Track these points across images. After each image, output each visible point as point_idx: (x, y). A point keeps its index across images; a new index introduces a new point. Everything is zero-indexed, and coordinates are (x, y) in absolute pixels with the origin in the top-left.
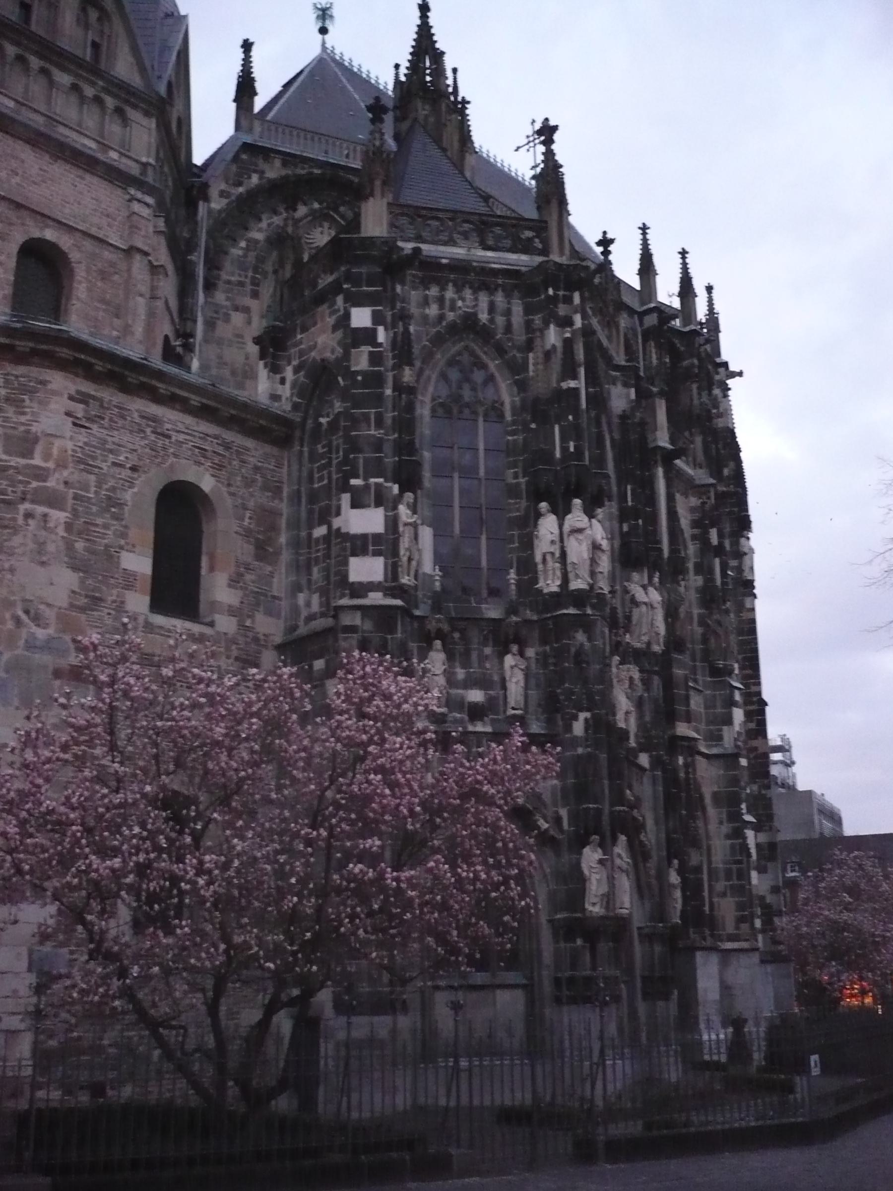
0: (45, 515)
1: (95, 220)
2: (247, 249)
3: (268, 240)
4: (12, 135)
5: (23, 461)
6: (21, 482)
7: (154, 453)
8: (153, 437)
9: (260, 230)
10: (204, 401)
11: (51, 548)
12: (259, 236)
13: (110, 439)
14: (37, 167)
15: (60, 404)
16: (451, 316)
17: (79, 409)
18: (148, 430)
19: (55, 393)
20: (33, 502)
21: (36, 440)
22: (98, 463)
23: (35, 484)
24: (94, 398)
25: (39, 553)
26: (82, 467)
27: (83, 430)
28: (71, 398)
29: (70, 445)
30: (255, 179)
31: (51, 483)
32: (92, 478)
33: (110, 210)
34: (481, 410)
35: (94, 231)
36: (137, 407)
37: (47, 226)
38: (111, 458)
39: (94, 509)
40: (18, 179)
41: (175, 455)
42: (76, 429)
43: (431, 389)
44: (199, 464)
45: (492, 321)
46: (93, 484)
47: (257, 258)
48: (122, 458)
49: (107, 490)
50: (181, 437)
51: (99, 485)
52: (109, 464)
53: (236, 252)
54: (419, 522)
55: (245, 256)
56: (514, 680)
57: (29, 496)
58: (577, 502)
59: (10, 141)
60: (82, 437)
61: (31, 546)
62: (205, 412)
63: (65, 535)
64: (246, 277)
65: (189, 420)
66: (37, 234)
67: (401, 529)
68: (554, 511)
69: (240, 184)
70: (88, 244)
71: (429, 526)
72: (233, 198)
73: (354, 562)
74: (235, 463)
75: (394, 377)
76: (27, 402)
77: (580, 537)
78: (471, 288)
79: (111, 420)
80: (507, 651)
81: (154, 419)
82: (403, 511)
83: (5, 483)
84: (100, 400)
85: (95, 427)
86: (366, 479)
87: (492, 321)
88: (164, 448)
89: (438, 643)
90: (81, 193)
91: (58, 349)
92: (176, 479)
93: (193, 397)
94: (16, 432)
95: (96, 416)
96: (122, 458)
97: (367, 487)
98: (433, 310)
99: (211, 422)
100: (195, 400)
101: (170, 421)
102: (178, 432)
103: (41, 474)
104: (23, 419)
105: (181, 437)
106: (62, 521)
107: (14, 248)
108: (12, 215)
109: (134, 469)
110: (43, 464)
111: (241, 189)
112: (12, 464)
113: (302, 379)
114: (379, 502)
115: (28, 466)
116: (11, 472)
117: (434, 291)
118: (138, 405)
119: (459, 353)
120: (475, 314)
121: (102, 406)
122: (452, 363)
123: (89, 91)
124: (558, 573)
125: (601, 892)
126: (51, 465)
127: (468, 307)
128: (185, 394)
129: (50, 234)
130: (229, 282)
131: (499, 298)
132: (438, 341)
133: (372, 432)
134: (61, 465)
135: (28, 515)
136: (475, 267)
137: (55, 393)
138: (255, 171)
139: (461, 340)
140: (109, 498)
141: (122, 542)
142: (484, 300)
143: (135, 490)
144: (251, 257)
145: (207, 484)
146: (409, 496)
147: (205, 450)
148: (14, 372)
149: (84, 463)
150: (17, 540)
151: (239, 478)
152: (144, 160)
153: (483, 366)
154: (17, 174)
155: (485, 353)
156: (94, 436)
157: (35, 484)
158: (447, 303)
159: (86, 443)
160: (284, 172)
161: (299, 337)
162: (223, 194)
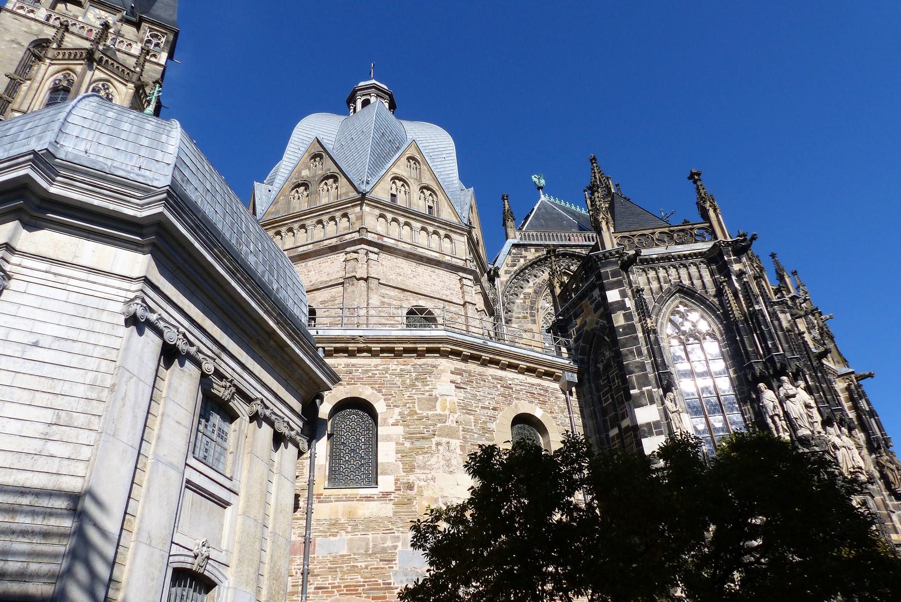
0: (448, 443)
1: (445, 292)
2: (525, 297)
3: (535, 292)
5: (430, 413)
6: (431, 425)
8: (502, 389)
9: (530, 287)
10: (528, 364)
11: (454, 462)
12: (531, 291)
14: (410, 270)
15: (448, 377)
16: (666, 286)
17: (458, 378)
18: (499, 386)
19: (443, 371)
20: (439, 436)
21: (437, 399)
24: (465, 371)
25: (448, 466)
26: (464, 411)
27: (462, 390)
28: (452, 373)
29: (456, 400)
30: (522, 261)
31: (448, 423)
32: (472, 417)
33: (451, 286)
35: (444, 298)
36: (490, 373)
37: (420, 299)
38: (480, 405)
39: (476, 436)
40: (401, 277)
41: (517, 399)
42: (459, 390)
44: (531, 402)
47: (531, 303)
48: (487, 404)
51: (476, 422)
52: (480, 408)
53: (519, 301)
54: (680, 410)
55: (525, 302)
57: (436, 433)
60: (461, 394)
61: (443, 462)
63: (462, 453)
64: (527, 313)
67: (671, 415)
68: (770, 387)
69: (515, 265)
70: (441, 304)
72: (513, 273)
73: (644, 441)
74: (552, 399)
75: (642, 326)
76: (428, 378)
81: (501, 379)
82: (668, 403)
83: (422, 427)
84: (469, 372)
85: (468, 387)
87: (692, 283)
90: (435, 279)
91: (440, 345)
94: (423, 396)
95: (468, 381)
97: (642, 393)
101: (510, 379)
103: (442, 419)
104: (427, 388)
105: (518, 388)
106: (458, 444)
109: (494, 409)
110: (442, 413)
111: (516, 268)
112: (425, 414)
113: (581, 344)
114: (652, 402)
115: (434, 415)
116: (424, 420)
118: (492, 371)
121: (470, 375)
123: (431, 229)
126: (447, 412)
127: (675, 279)
129: (423, 303)
130: (519, 318)
131: (693, 269)
134: (453, 412)
137: (443, 371)
138: (521, 257)
142: (683, 272)
143: (498, 421)
144: (528, 302)
148: (419, 363)
149: (466, 409)
150: (434, 460)
151: (556, 408)
152: (464, 258)
157: (439, 425)
158: (662, 280)
160: (537, 255)
161: (574, 321)
162: (506, 272)
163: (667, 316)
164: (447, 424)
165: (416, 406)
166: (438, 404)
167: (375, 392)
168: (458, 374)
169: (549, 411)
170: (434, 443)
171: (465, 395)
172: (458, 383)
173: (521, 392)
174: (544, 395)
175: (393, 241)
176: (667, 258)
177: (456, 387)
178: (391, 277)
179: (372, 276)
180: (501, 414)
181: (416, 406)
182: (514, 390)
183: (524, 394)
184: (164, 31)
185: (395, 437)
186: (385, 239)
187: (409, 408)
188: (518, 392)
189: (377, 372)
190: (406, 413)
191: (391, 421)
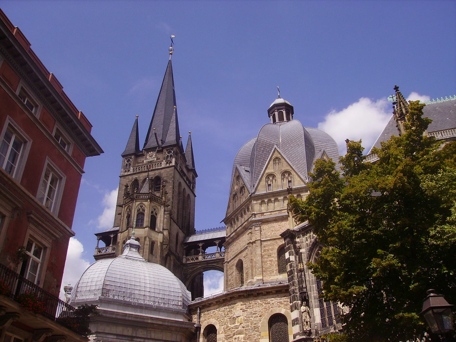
0: (238, 337)
5: (233, 325)
7: (265, 310)
13: (253, 311)
14: (278, 226)
18: (263, 304)
20: (236, 335)
22: (251, 318)
23: (236, 330)
27: (246, 312)
32: (250, 323)
46: (250, 325)
49: (254, 325)
60: (245, 314)
71: (318, 307)
79: (252, 306)
83: (230, 332)
85: (248, 310)
86: (293, 303)
88: (269, 307)
95: (248, 307)
96: (257, 315)
97: (293, 304)
103: (237, 327)
107: (276, 251)
108: (273, 242)
133: (293, 288)
135: (235, 339)
139: (317, 245)
140: (255, 327)
141: (260, 337)
143: (262, 322)
145: (283, 312)
147: (282, 302)
154: (273, 231)
156: (248, 312)
157: (236, 330)
158: (312, 236)
159: (246, 315)
164: (239, 329)
165: (229, 324)
166: (236, 320)
167: (216, 321)
168: (244, 305)
170: (234, 338)
171: (247, 314)
172: (243, 309)
174: (287, 301)
177: (243, 311)
180: (263, 318)
181: (229, 324)
182: (271, 303)
183: (276, 304)
184: (171, 148)
185: (222, 338)
187: (226, 325)
188: (273, 304)
189: (216, 312)
190: (225, 327)
191: (221, 332)
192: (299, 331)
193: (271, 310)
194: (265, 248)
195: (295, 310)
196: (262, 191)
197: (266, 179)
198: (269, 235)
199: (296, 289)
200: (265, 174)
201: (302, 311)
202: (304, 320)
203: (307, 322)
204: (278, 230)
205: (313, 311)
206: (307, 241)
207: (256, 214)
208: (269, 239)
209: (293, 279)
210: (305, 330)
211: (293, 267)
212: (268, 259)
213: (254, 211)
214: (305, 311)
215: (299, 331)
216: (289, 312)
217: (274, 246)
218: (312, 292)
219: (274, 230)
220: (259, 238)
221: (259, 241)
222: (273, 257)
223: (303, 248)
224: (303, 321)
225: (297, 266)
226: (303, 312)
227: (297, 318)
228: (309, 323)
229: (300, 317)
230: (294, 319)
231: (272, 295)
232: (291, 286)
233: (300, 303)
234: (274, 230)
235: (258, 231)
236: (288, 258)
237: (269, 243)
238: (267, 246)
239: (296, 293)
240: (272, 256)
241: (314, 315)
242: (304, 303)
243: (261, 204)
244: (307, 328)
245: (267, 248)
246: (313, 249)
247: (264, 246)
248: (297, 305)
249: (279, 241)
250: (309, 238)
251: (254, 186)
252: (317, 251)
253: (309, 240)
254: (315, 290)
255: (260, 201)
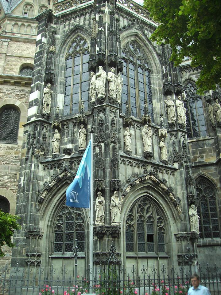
4: (19, 42)
10: (15, 80)
14: (26, 47)
16: (71, 27)
34: (81, 52)
37: (28, 60)
40: (20, 51)
43: (66, 52)
45: (84, 24)
50: (9, 92)
56: (80, 137)
58: (100, 67)
59: (18, 43)
62: (16, 83)
65: (12, 87)
66: (25, 62)
77: (100, 78)
78: (78, 17)
80: (80, 128)
87: (84, 24)
88: (3, 96)
89: (56, 131)
92: (6, 104)
93: (11, 80)
97: (35, 85)
98: (67, 28)
99: (20, 86)
100: (12, 81)
102: (8, 91)
105: (9, 92)
117: (67, 22)
119: (76, 38)
120: (79, 23)
122: (73, 43)
124: (95, 95)
125: (100, 216)
127: (77, 23)
128: (8, 80)
132: (67, 36)
136: (78, 10)
139: (76, 33)
142: (82, 18)
145: (18, 104)
146: (49, 85)
147: (18, 94)
153: (83, 39)
155: (83, 34)
163: (69, 43)
169: (25, 102)
173: (10, 95)
175: (20, 35)
176: (74, 12)
178: (15, 52)
179: (3, 52)
183: (12, 95)
186: (15, 34)
188: (8, 94)
192: (36, 113)
193: (5, 100)
194: (8, 63)
195: (36, 90)
196: (18, 14)
197: (24, 6)
198: (15, 53)
199: (42, 71)
200: (24, 2)
201: (45, 92)
202: (45, 101)
203: (48, 105)
204: (25, 51)
205: (57, 96)
206: (65, 28)
207: (7, 32)
208: (15, 55)
209: (41, 60)
210: (44, 112)
211: (43, 48)
212: (9, 72)
213: (5, 29)
214: (47, 93)
215: (36, 113)
216: (24, 105)
217: (18, 62)
218: (59, 78)
219: (21, 49)
220: (5, 52)
221: (4, 55)
222: (14, 72)
223: (59, 34)
224: (44, 103)
225: (49, 48)
226: (45, 94)
227: (37, 99)
228: (50, 106)
229: (40, 99)
230: (33, 101)
231: (9, 85)
232: (36, 67)
233: (44, 84)
234: (21, 49)
235: (5, 46)
236: (39, 40)
237: (14, 59)
238: (11, 61)
239: (41, 74)
240: (14, 70)
241: (56, 100)
242: (49, 85)
243: (14, 25)
244: (46, 111)
245: (11, 63)
246: (70, 36)
247: (8, 60)
248: (40, 86)
249: (24, 60)
250: (67, 26)
251: (10, 9)
252: (74, 39)
253: (67, 28)
254: (63, 75)
255: (13, 23)
